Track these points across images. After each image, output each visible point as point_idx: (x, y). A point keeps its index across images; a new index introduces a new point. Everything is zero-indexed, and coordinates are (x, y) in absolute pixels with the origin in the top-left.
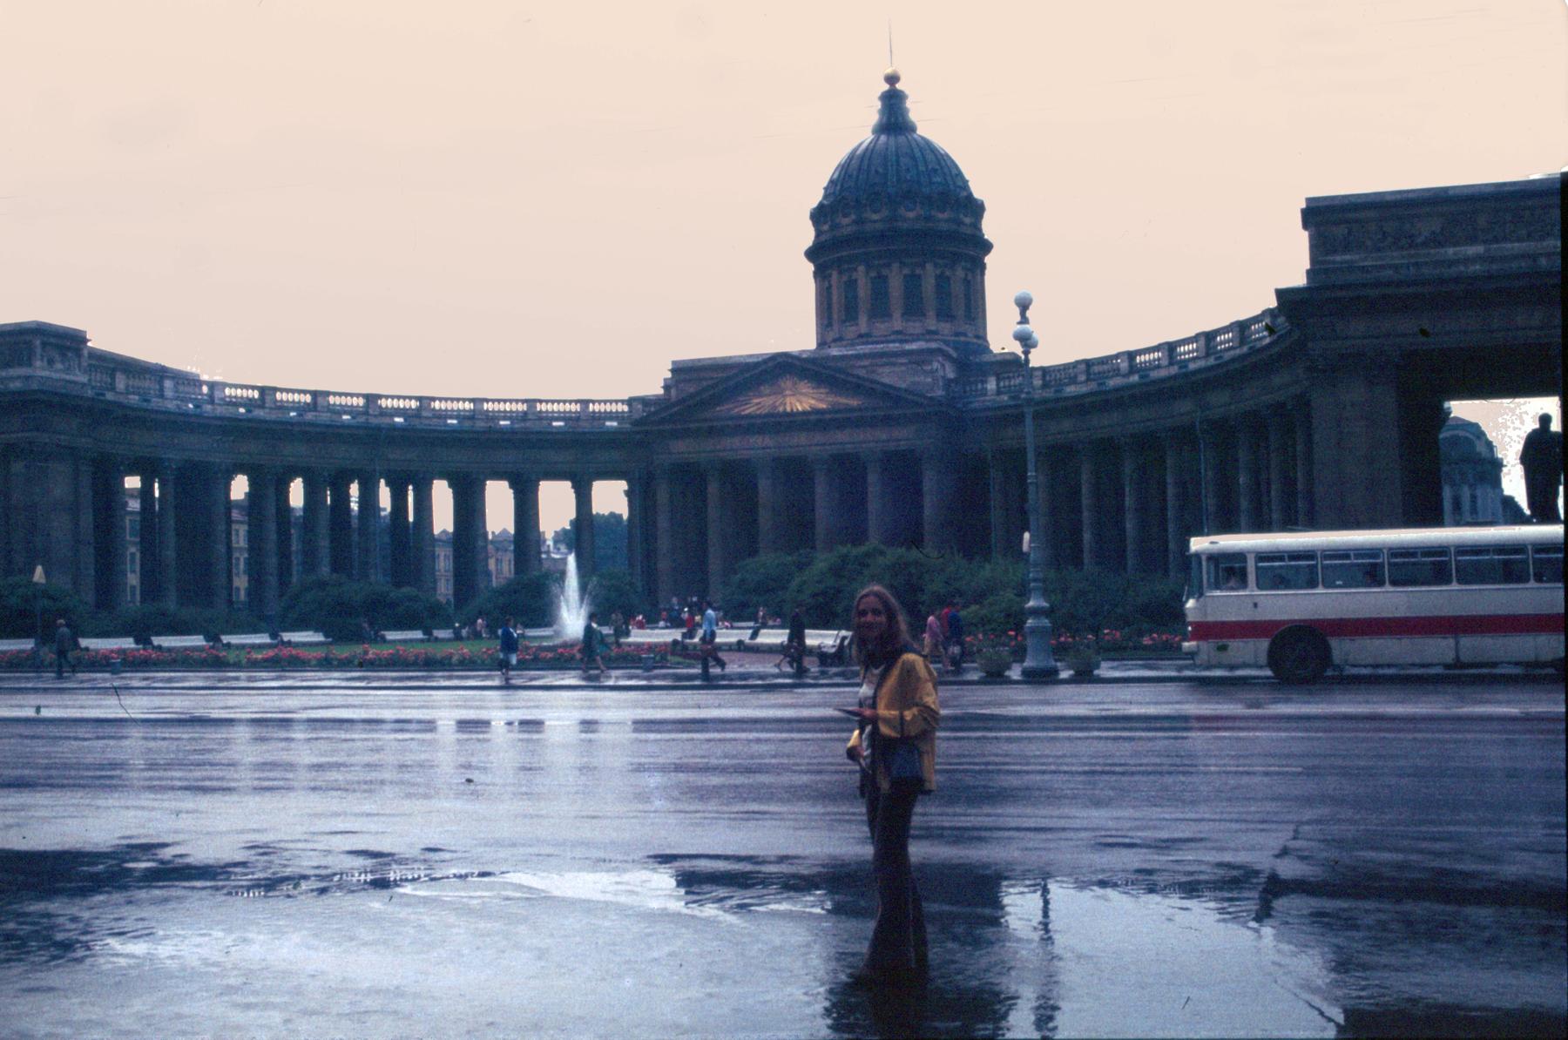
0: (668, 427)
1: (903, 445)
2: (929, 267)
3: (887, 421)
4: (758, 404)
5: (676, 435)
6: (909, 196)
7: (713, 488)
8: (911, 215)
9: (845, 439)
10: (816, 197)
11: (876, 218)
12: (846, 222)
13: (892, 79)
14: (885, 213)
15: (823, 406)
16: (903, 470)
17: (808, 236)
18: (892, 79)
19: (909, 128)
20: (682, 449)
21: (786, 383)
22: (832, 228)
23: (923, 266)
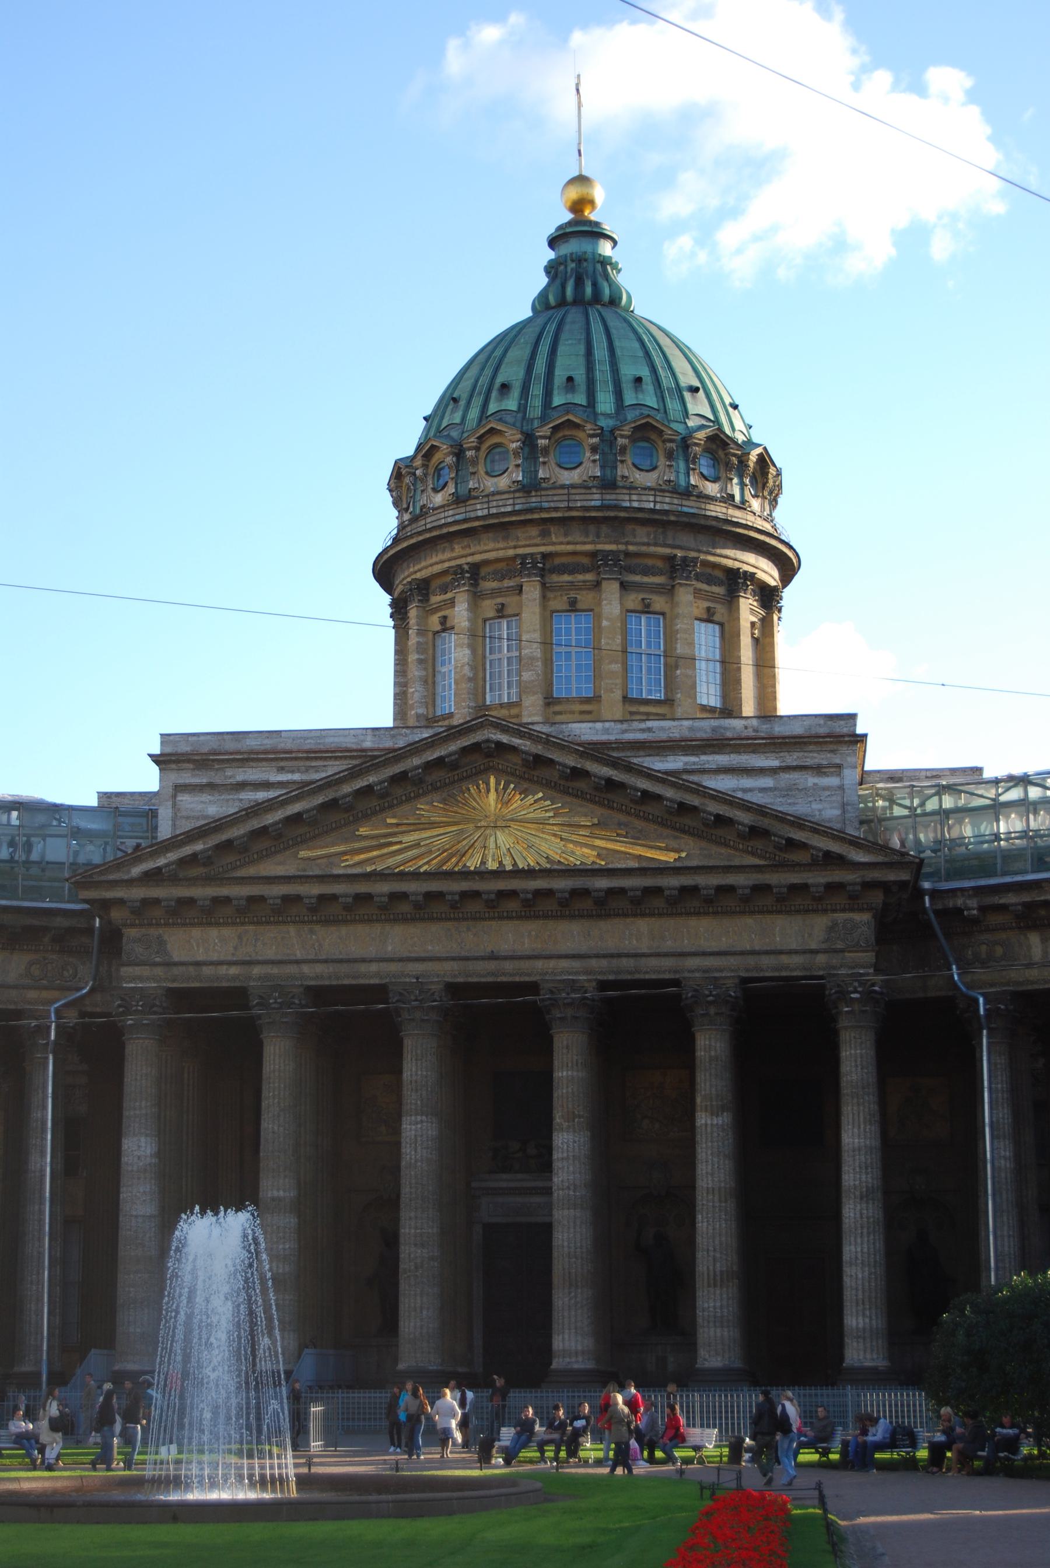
1: (794, 965)
2: (685, 596)
4: (415, 842)
5: (182, 912)
7: (279, 1060)
8: (648, 479)
9: (644, 945)
11: (571, 474)
12: (499, 483)
17: (380, 524)
18: (578, 206)
21: (490, 797)
22: (458, 500)
23: (669, 591)
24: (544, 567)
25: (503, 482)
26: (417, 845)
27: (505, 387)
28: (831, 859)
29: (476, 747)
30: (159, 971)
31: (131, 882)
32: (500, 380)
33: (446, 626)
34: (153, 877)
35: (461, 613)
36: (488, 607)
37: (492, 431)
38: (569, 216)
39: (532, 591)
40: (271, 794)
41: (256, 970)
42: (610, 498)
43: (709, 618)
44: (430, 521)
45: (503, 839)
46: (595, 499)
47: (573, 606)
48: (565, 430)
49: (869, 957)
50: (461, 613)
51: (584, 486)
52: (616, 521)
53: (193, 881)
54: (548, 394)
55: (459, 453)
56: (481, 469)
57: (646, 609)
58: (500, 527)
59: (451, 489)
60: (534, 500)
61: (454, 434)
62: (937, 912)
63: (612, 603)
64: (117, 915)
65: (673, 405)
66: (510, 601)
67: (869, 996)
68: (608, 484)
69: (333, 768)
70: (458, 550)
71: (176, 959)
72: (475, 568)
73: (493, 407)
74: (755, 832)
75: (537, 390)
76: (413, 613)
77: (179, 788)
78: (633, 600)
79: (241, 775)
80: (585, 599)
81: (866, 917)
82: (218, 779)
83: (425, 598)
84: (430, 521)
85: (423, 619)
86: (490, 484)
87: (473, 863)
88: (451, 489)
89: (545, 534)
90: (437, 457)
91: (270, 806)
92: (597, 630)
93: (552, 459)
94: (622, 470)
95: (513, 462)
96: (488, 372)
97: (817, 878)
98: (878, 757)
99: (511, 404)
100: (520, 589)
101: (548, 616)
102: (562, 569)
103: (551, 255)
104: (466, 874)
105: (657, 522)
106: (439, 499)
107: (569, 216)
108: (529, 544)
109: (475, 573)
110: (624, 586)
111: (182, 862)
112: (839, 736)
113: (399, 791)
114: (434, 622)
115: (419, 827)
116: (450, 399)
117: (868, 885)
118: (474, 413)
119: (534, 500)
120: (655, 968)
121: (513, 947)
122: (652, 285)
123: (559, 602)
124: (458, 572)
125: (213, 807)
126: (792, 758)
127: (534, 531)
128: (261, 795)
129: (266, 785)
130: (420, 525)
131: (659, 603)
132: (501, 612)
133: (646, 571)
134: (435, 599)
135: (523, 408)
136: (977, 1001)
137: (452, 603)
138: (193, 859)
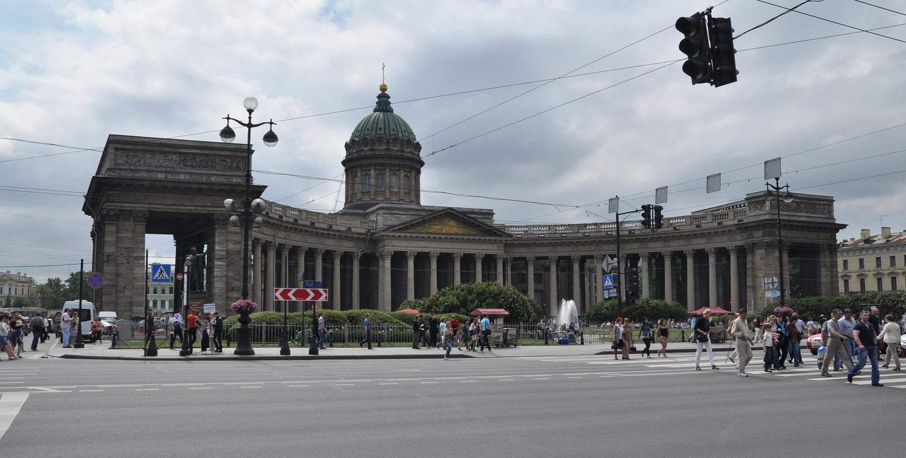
0: (397, 234)
3: (490, 242)
14: (398, 148)
19: (391, 111)
22: (371, 150)
23: (410, 172)
24: (391, 165)
35: (372, 172)
36: (378, 172)
38: (380, 92)
39: (388, 170)
45: (448, 228)
48: (396, 139)
50: (372, 172)
51: (398, 151)
58: (381, 157)
66: (383, 172)
68: (402, 151)
74: (489, 230)
76: (359, 171)
80: (397, 173)
92: (399, 179)
97: (498, 239)
98: (495, 217)
101: (391, 175)
104: (442, 234)
107: (380, 92)
108: (387, 161)
109: (376, 165)
112: (490, 214)
118: (374, 132)
120: (472, 252)
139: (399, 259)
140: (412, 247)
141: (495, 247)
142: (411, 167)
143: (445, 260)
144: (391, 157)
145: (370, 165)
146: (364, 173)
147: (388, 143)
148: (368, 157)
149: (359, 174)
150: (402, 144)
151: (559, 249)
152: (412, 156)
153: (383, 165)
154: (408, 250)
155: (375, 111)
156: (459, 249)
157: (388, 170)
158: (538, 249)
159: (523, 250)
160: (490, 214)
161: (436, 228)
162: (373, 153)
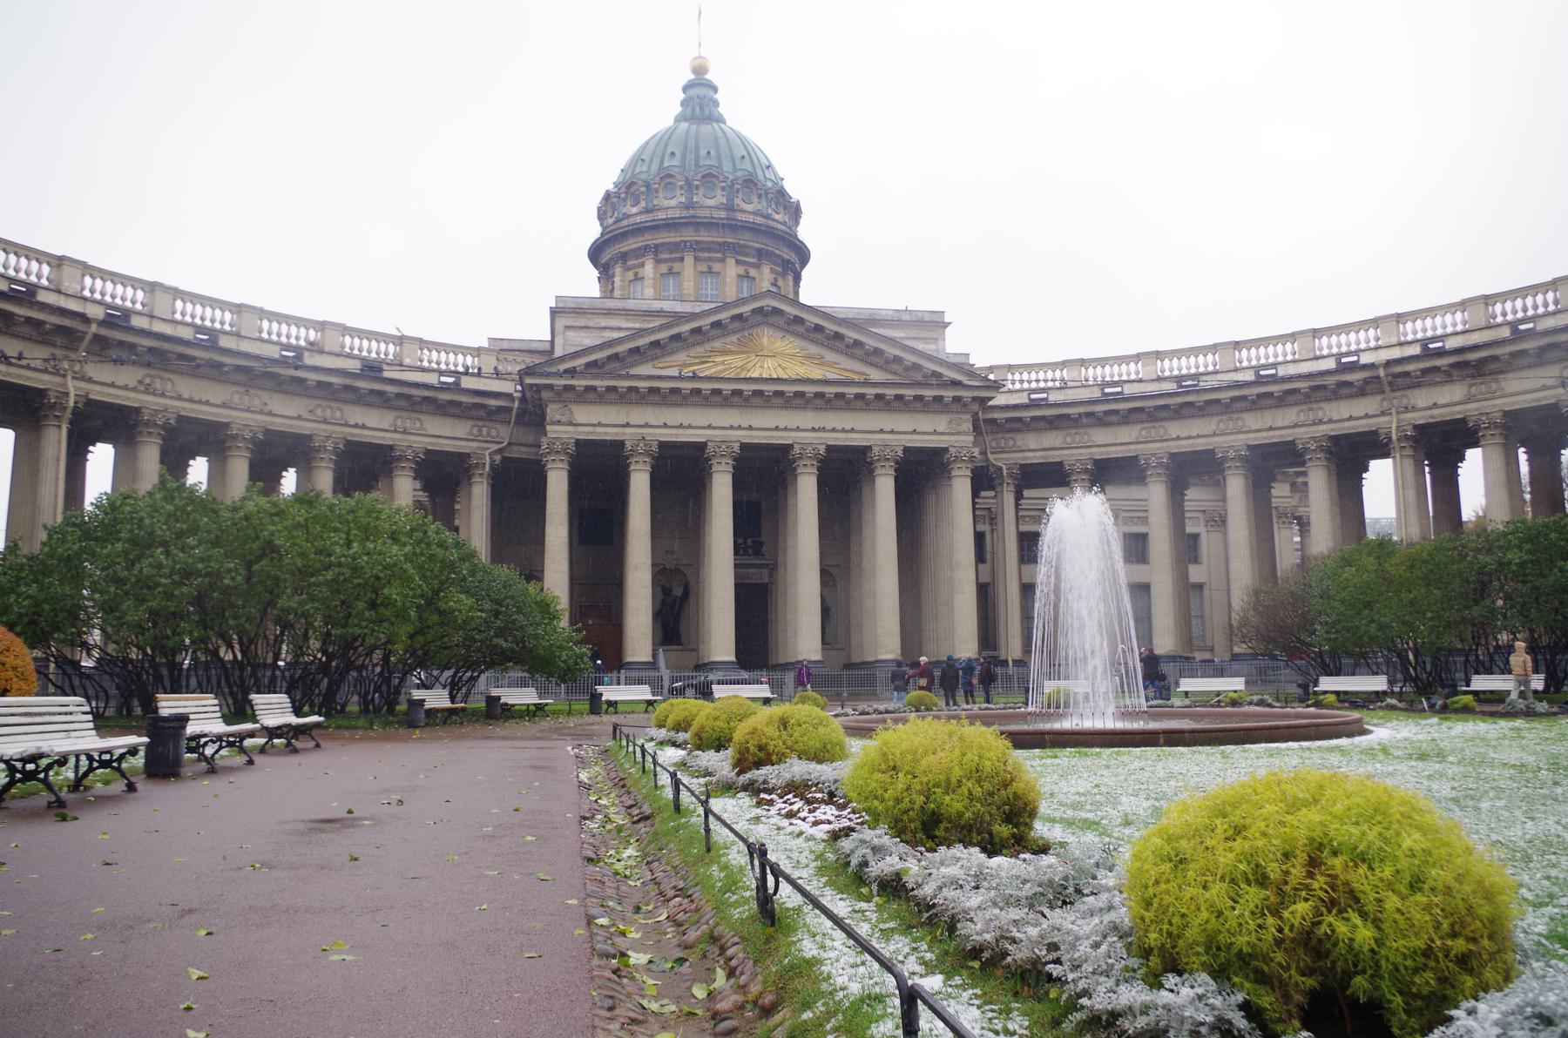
0: (580, 383)
2: (766, 270)
4: (725, 363)
6: (750, 183)
7: (640, 485)
10: (608, 180)
11: (711, 202)
12: (671, 204)
13: (700, 70)
15: (816, 373)
16: (920, 474)
18: (700, 70)
19: (721, 120)
20: (596, 422)
21: (768, 338)
22: (648, 211)
23: (757, 266)
24: (697, 247)
25: (673, 203)
26: (723, 363)
27: (673, 154)
28: (955, 384)
29: (760, 311)
30: (570, 428)
31: (558, 375)
32: (670, 150)
33: (638, 278)
34: (571, 372)
35: (649, 269)
36: (664, 268)
37: (669, 176)
38: (692, 77)
39: (689, 259)
40: (622, 334)
41: (628, 430)
42: (732, 215)
43: (774, 284)
44: (632, 220)
45: (770, 363)
46: (723, 214)
47: (710, 271)
48: (710, 178)
49: (971, 438)
50: (649, 269)
51: (718, 208)
52: (734, 227)
53: (596, 377)
54: (697, 158)
55: (648, 185)
56: (661, 195)
57: (747, 276)
58: (671, 225)
59: (643, 204)
60: (692, 212)
61: (643, 177)
62: (987, 421)
63: (731, 270)
64: (545, 395)
65: (760, 173)
66: (677, 267)
67: (972, 459)
68: (730, 208)
69: (657, 323)
70: (647, 236)
71: (580, 421)
72: (657, 247)
73: (666, 164)
75: (691, 157)
76: (618, 270)
77: (567, 327)
78: (741, 270)
79: (604, 322)
80: (717, 267)
81: (968, 417)
82: (591, 324)
83: (625, 262)
84: (632, 220)
85: (622, 275)
86: (666, 203)
87: (755, 375)
88: (643, 204)
89: (697, 230)
90: (634, 188)
91: (619, 341)
92: (725, 283)
93: (701, 192)
94: (737, 201)
95: (678, 192)
96: (662, 145)
97: (948, 394)
99: (676, 162)
100: (682, 259)
102: (702, 250)
103: (682, 96)
105: (754, 229)
106: (635, 210)
107: (692, 77)
108: (688, 236)
110: (738, 262)
111: (588, 365)
112: (935, 324)
113: (715, 332)
114: (630, 275)
115: (724, 352)
116: (638, 159)
117: (974, 399)
118: (655, 167)
119: (692, 212)
120: (856, 440)
121: (766, 427)
122: (742, 114)
123: (703, 267)
124: (646, 248)
125: (588, 340)
126: (912, 334)
127: (691, 229)
128: (616, 335)
129: (620, 329)
130: (625, 223)
131: (753, 273)
132: (671, 272)
133: (747, 255)
134: (630, 263)
135: (683, 165)
136: (1000, 469)
137: (642, 265)
138: (594, 364)
139: (599, 472)
140: (643, 427)
141: (941, 422)
142: (760, 254)
143: (764, 475)
144: (696, 224)
145: (640, 253)
146: (630, 275)
147: (690, 187)
148: (639, 230)
149: (617, 279)
150: (730, 189)
151: (1174, 428)
152: (759, 220)
153: (676, 247)
154: (628, 435)
155: (678, 120)
156: (808, 431)
157: (689, 259)
158: (1100, 436)
159: (1052, 439)
160: (935, 324)
161: (725, 363)
162: (649, 217)
